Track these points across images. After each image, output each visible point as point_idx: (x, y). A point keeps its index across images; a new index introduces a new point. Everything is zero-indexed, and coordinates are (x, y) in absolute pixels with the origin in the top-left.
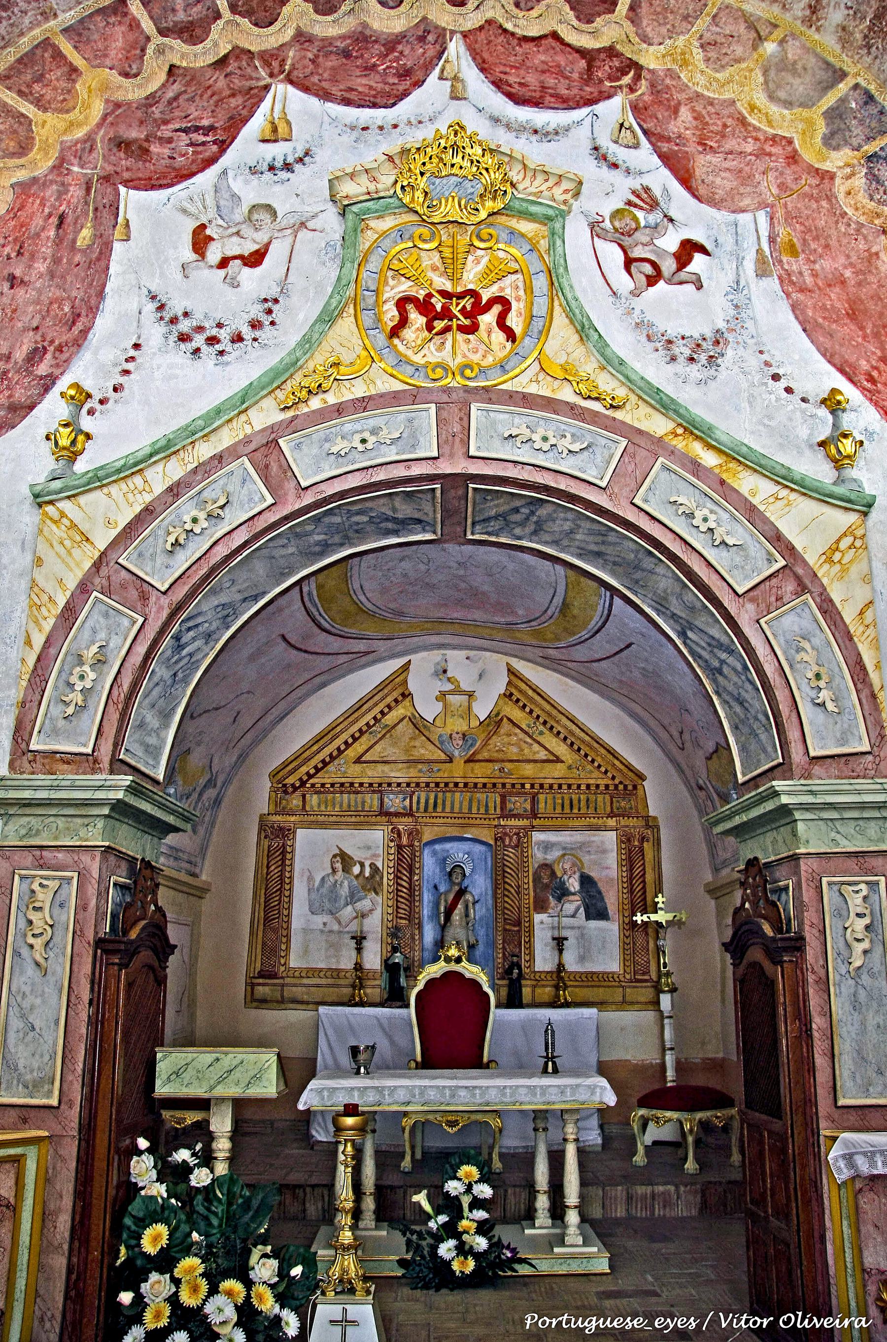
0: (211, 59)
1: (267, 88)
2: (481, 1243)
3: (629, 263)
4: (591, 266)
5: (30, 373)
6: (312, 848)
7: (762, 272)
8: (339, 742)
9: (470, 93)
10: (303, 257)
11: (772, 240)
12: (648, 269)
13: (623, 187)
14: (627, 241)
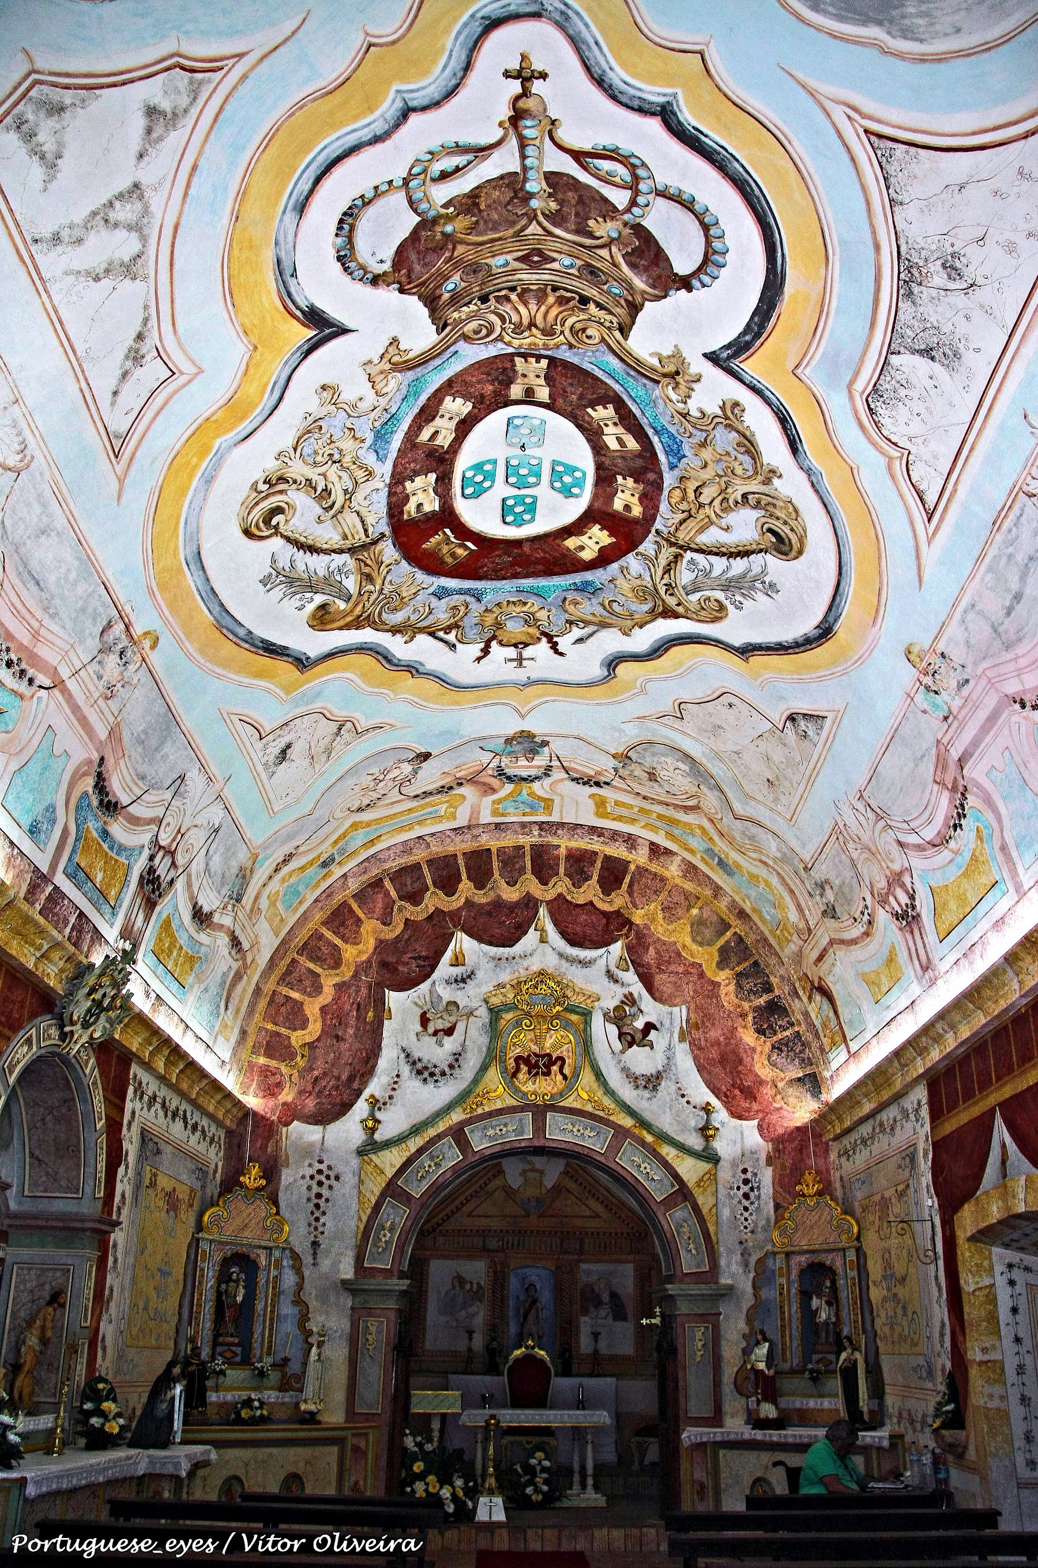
0: (425, 915)
1: (452, 934)
2: (545, 1488)
3: (621, 1035)
4: (604, 1034)
5: (349, 1087)
6: (440, 1272)
7: (682, 1039)
8: (457, 1202)
9: (550, 939)
10: (473, 1032)
11: (688, 1021)
12: (629, 1038)
13: (619, 992)
14: (621, 1023)
